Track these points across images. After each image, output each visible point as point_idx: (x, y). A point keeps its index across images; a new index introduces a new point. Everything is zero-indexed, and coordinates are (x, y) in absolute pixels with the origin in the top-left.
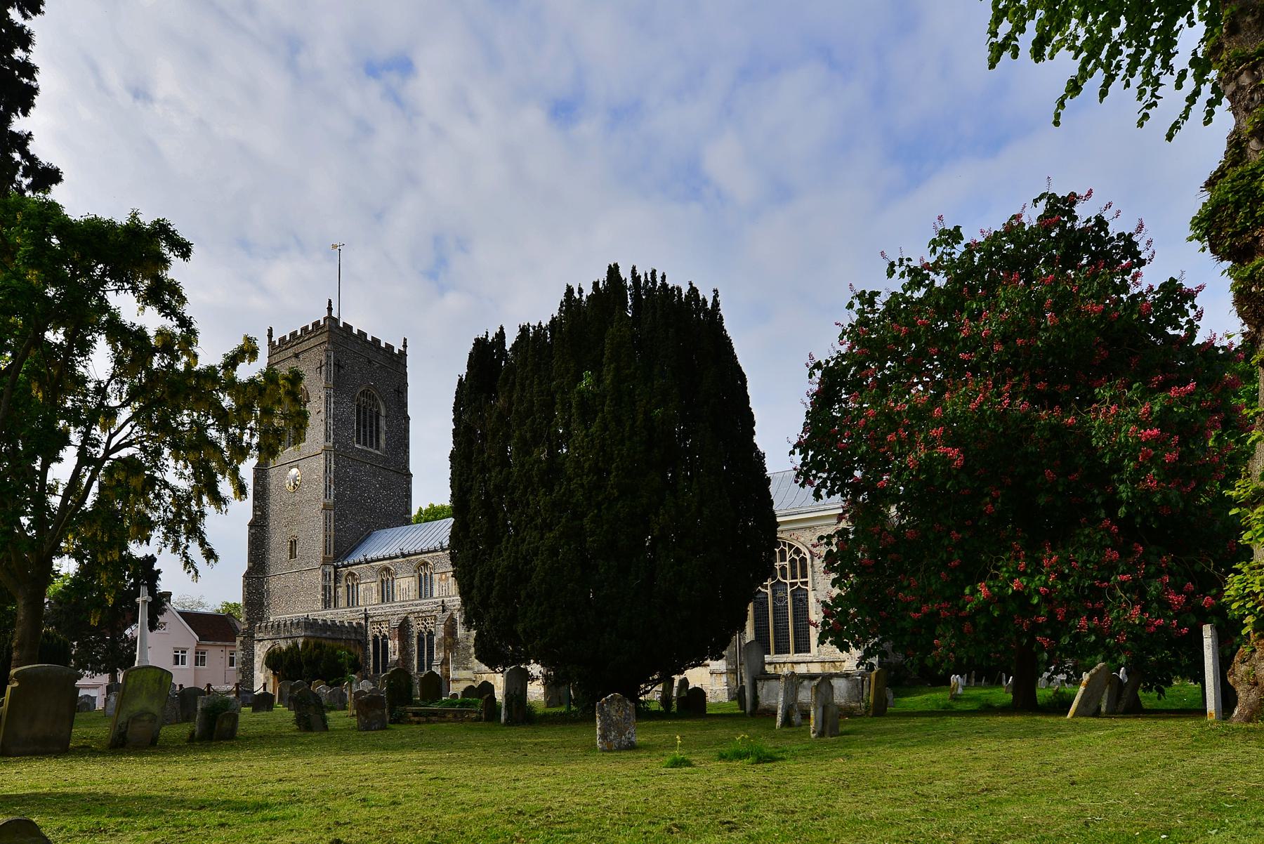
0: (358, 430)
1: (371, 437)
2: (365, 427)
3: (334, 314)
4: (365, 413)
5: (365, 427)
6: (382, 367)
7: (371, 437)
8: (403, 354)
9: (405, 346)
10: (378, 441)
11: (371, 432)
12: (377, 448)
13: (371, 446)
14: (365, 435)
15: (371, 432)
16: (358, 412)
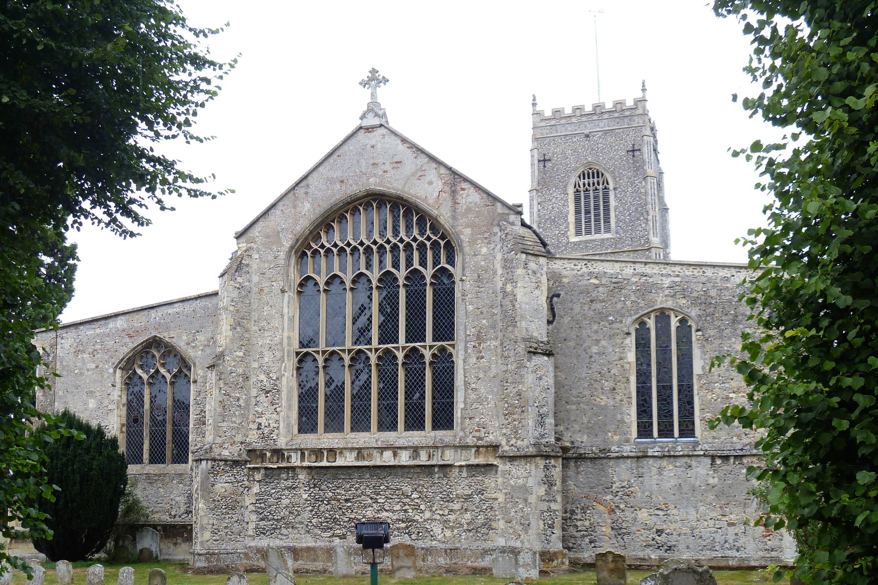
0: (578, 221)
1: (597, 220)
2: (588, 212)
3: (538, 108)
4: (587, 197)
5: (588, 212)
6: (606, 132)
7: (597, 220)
8: (641, 102)
9: (644, 90)
10: (607, 220)
11: (597, 215)
12: (608, 230)
13: (598, 231)
14: (588, 221)
15: (597, 215)
16: (577, 200)
